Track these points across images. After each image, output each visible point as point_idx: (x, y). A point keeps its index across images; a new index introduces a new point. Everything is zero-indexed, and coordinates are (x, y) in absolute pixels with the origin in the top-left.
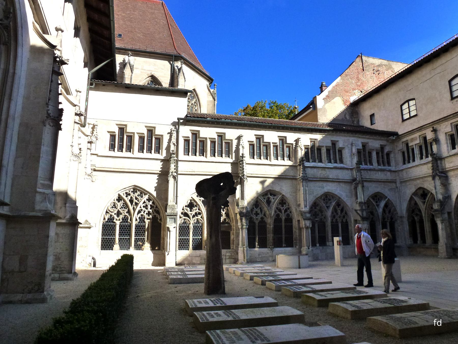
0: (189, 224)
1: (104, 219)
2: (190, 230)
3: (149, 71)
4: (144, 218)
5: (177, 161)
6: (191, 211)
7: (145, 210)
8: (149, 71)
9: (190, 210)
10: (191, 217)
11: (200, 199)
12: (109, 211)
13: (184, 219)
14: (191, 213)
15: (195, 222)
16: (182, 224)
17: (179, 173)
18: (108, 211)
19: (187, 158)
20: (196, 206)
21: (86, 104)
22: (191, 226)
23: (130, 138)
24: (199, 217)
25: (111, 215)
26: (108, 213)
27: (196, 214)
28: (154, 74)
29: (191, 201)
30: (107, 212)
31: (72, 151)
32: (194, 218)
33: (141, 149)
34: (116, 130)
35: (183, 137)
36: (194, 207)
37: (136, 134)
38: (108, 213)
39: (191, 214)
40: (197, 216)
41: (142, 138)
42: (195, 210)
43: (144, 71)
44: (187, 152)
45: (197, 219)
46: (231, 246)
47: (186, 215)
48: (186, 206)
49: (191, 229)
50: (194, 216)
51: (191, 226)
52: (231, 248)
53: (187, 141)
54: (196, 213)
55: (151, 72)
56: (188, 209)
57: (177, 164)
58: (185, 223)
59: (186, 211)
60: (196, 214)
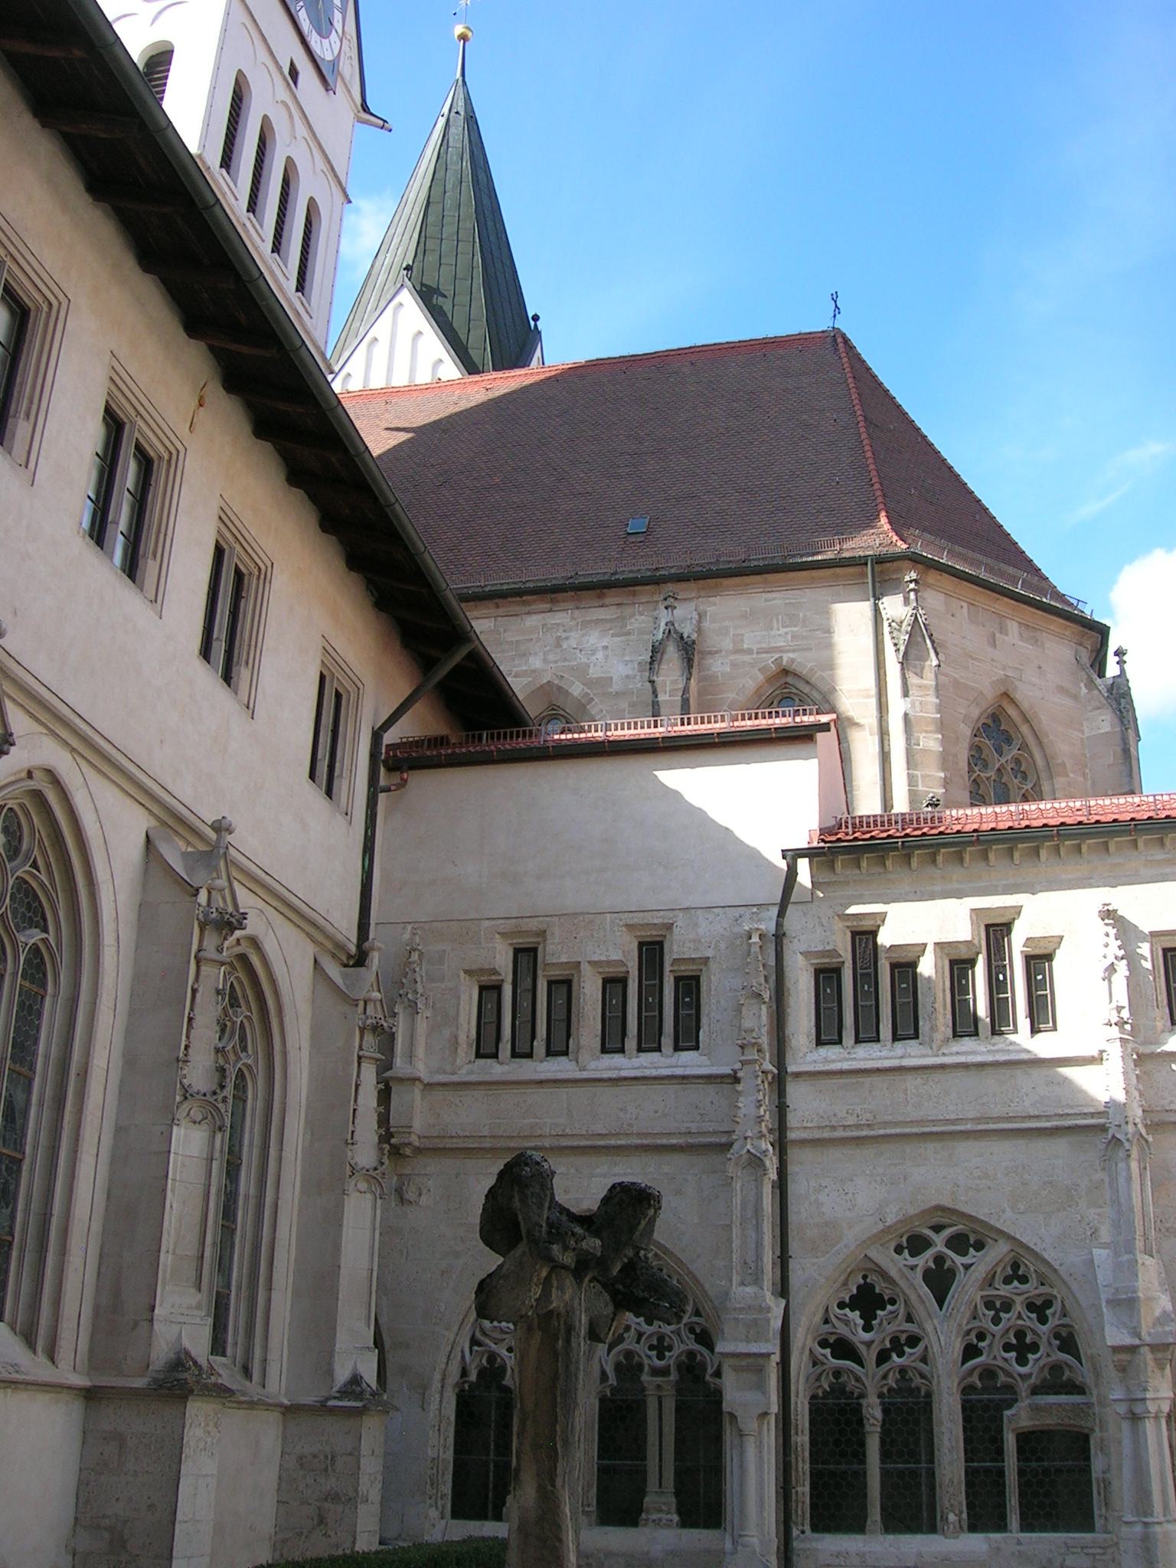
0: (862, 1396)
1: (464, 1373)
2: (868, 1428)
3: (768, 651)
4: (640, 1366)
5: (780, 1082)
6: (867, 1328)
7: (645, 1327)
8: (768, 651)
9: (862, 1322)
10: (870, 1356)
11: (912, 1261)
12: (484, 1333)
13: (837, 1373)
14: (867, 1336)
15: (891, 1381)
16: (823, 1398)
17: (792, 1135)
18: (478, 1335)
19: (832, 1057)
20: (893, 1302)
21: (366, 866)
22: (873, 1411)
23: (564, 986)
24: (909, 1358)
25: (492, 1357)
26: (479, 1344)
27: (897, 1346)
28: (793, 661)
29: (865, 1277)
30: (474, 1342)
31: (185, 1081)
32: (886, 1367)
33: (613, 1042)
34: (503, 960)
35: (806, 954)
36: (884, 1309)
37: (586, 968)
38: (479, 1344)
39: (869, 1344)
40: (901, 1354)
41: (614, 984)
42: (889, 1323)
43: (747, 658)
44: (827, 1033)
45: (903, 1371)
46: (1096, 1512)
47: (843, 1348)
48: (841, 1305)
49: (872, 1421)
50: (883, 1357)
51: (873, 1411)
52: (1099, 1523)
53: (826, 975)
54: (895, 1340)
55: (776, 656)
56: (855, 1316)
57: (781, 1093)
58: (838, 1390)
59: (843, 1330)
60: (897, 1346)
